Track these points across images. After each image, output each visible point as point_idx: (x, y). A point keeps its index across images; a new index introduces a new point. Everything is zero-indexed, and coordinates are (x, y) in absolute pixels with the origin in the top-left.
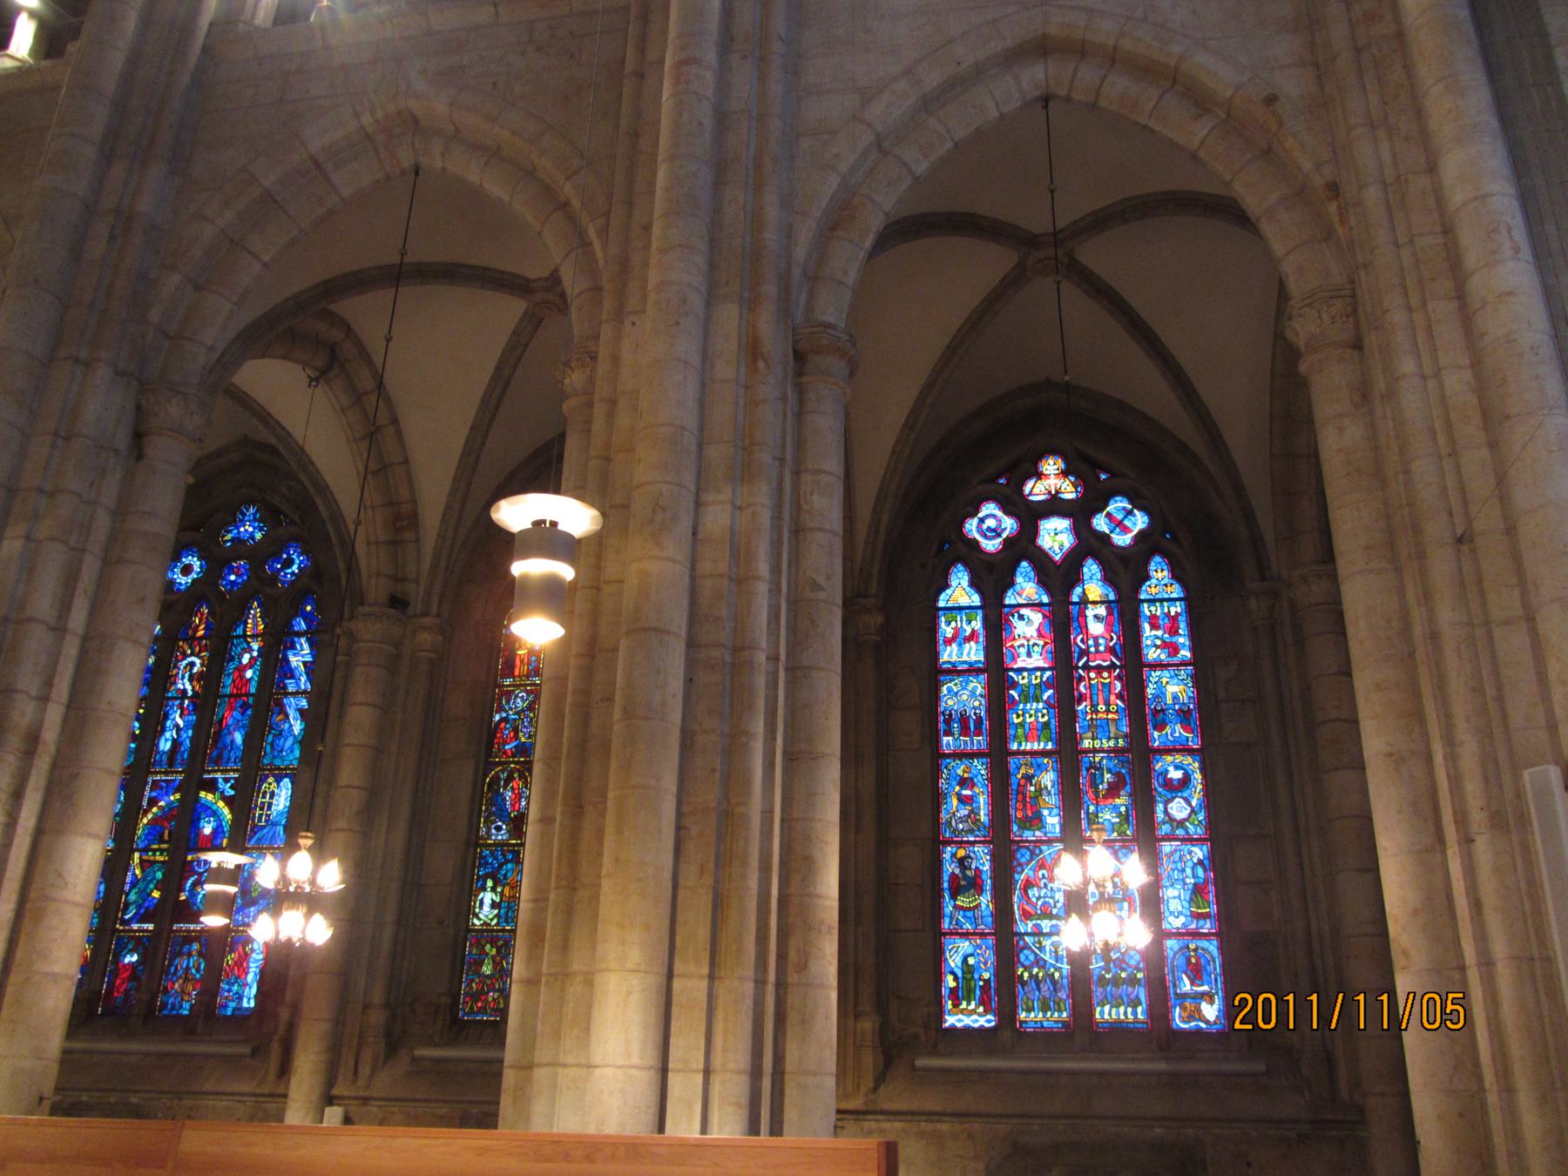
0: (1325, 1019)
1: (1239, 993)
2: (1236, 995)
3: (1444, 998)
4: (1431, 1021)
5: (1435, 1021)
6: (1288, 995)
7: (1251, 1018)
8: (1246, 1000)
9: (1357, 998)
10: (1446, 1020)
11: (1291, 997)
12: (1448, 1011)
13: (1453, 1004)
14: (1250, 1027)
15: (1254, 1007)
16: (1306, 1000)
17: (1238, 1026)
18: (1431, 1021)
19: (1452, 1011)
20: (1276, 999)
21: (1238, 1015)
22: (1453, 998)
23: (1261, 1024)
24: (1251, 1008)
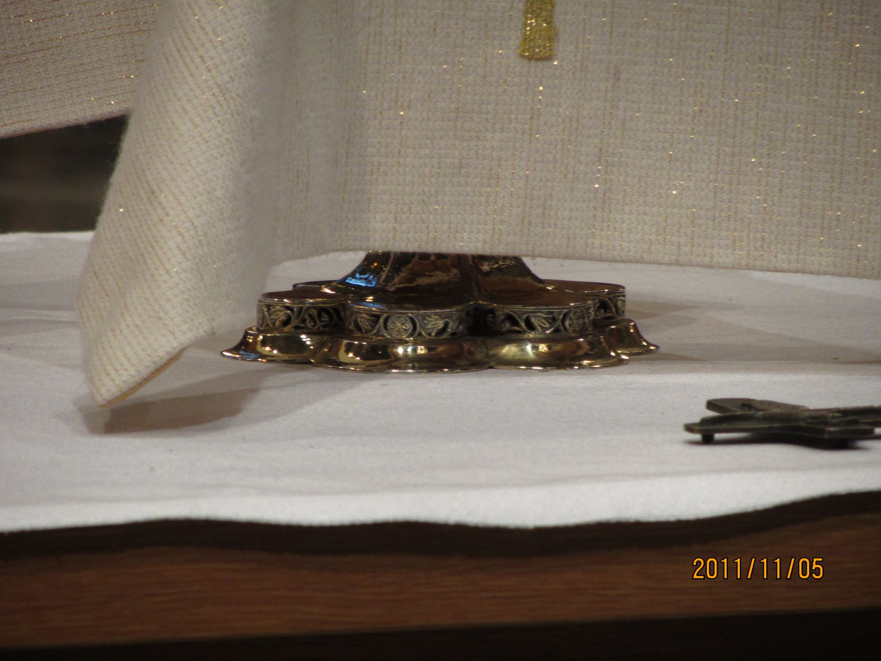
0: (745, 571)
1: (696, 558)
2: (695, 560)
5: (806, 574)
6: (724, 559)
7: (703, 572)
8: (700, 562)
9: (763, 561)
11: (725, 561)
12: (814, 568)
13: (816, 564)
14: (702, 577)
16: (734, 562)
17: (695, 577)
19: (816, 568)
20: (717, 561)
21: (696, 570)
22: (817, 561)
23: (709, 576)
24: (703, 567)
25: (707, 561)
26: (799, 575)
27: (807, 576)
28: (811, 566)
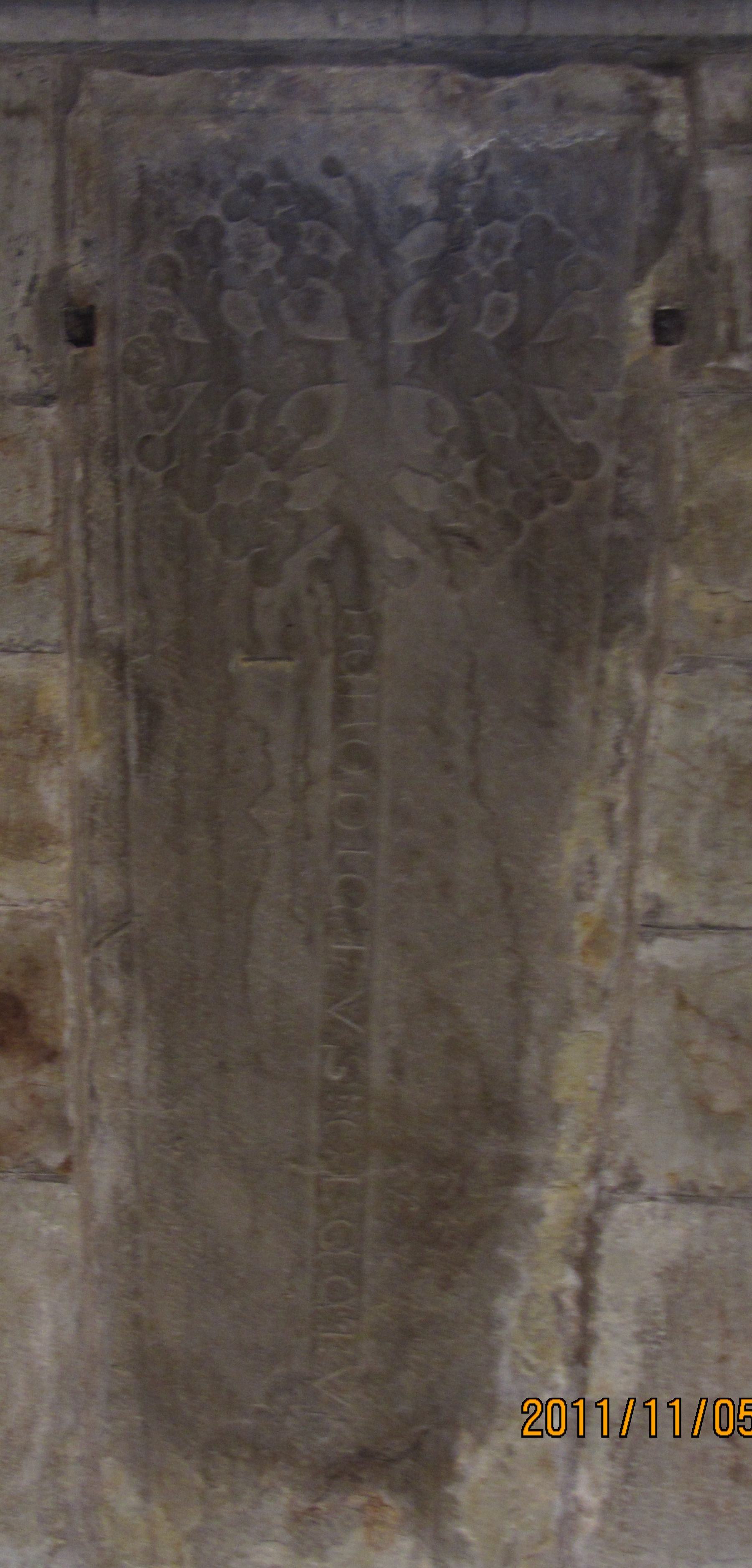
3: (737, 1404)
4: (724, 1427)
8: (536, 1407)
10: (739, 1427)
12: (741, 1418)
13: (746, 1410)
14: (539, 1433)
15: (544, 1414)
18: (724, 1427)
19: (745, 1417)
22: (747, 1405)
25: (547, 1404)
26: (715, 1430)
27: (729, 1431)
28: (737, 1413)
